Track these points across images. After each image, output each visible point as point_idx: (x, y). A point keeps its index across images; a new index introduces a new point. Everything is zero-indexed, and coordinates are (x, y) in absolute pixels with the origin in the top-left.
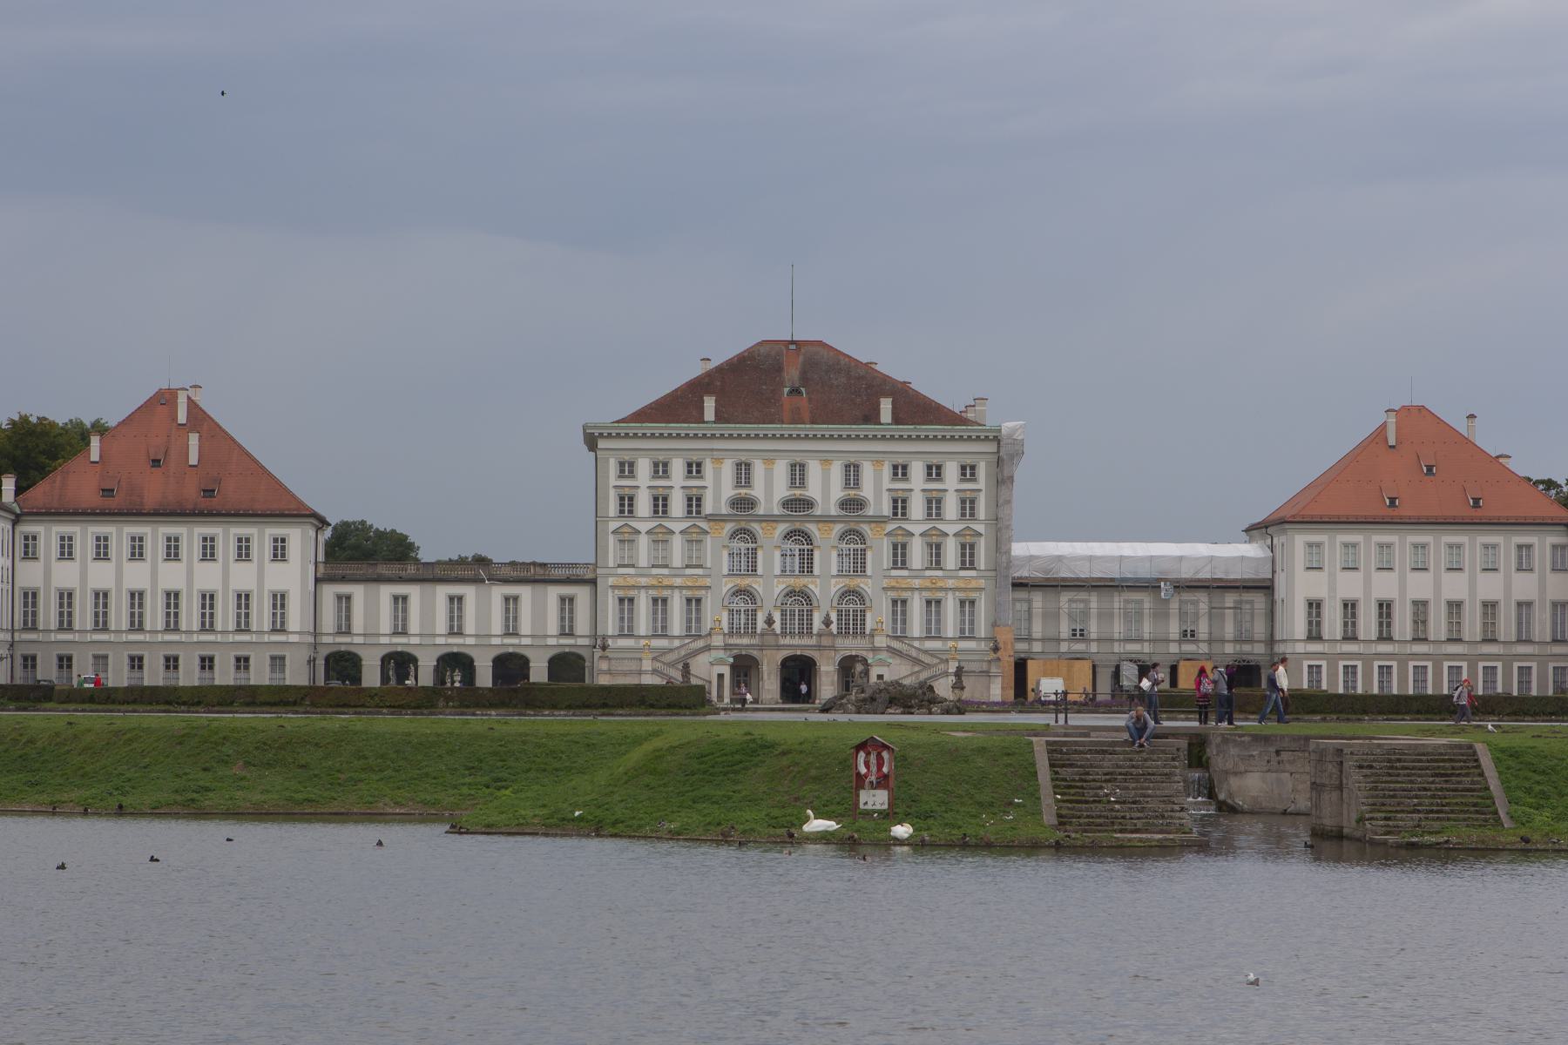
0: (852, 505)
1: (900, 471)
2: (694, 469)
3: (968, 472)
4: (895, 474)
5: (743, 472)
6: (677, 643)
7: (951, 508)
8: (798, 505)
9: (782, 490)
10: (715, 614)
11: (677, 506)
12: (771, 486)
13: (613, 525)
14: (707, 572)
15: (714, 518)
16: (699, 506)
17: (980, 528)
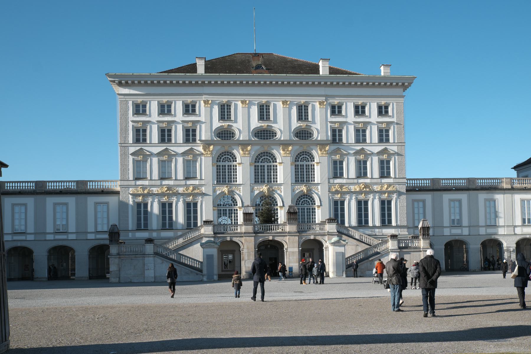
0: (303, 134)
1: (336, 110)
2: (189, 109)
3: (383, 110)
4: (333, 113)
5: (225, 112)
6: (180, 233)
7: (372, 134)
8: (265, 134)
9: (255, 123)
10: (206, 211)
11: (178, 134)
12: (245, 120)
13: (132, 150)
14: (203, 182)
15: (207, 144)
16: (194, 135)
17: (393, 149)
